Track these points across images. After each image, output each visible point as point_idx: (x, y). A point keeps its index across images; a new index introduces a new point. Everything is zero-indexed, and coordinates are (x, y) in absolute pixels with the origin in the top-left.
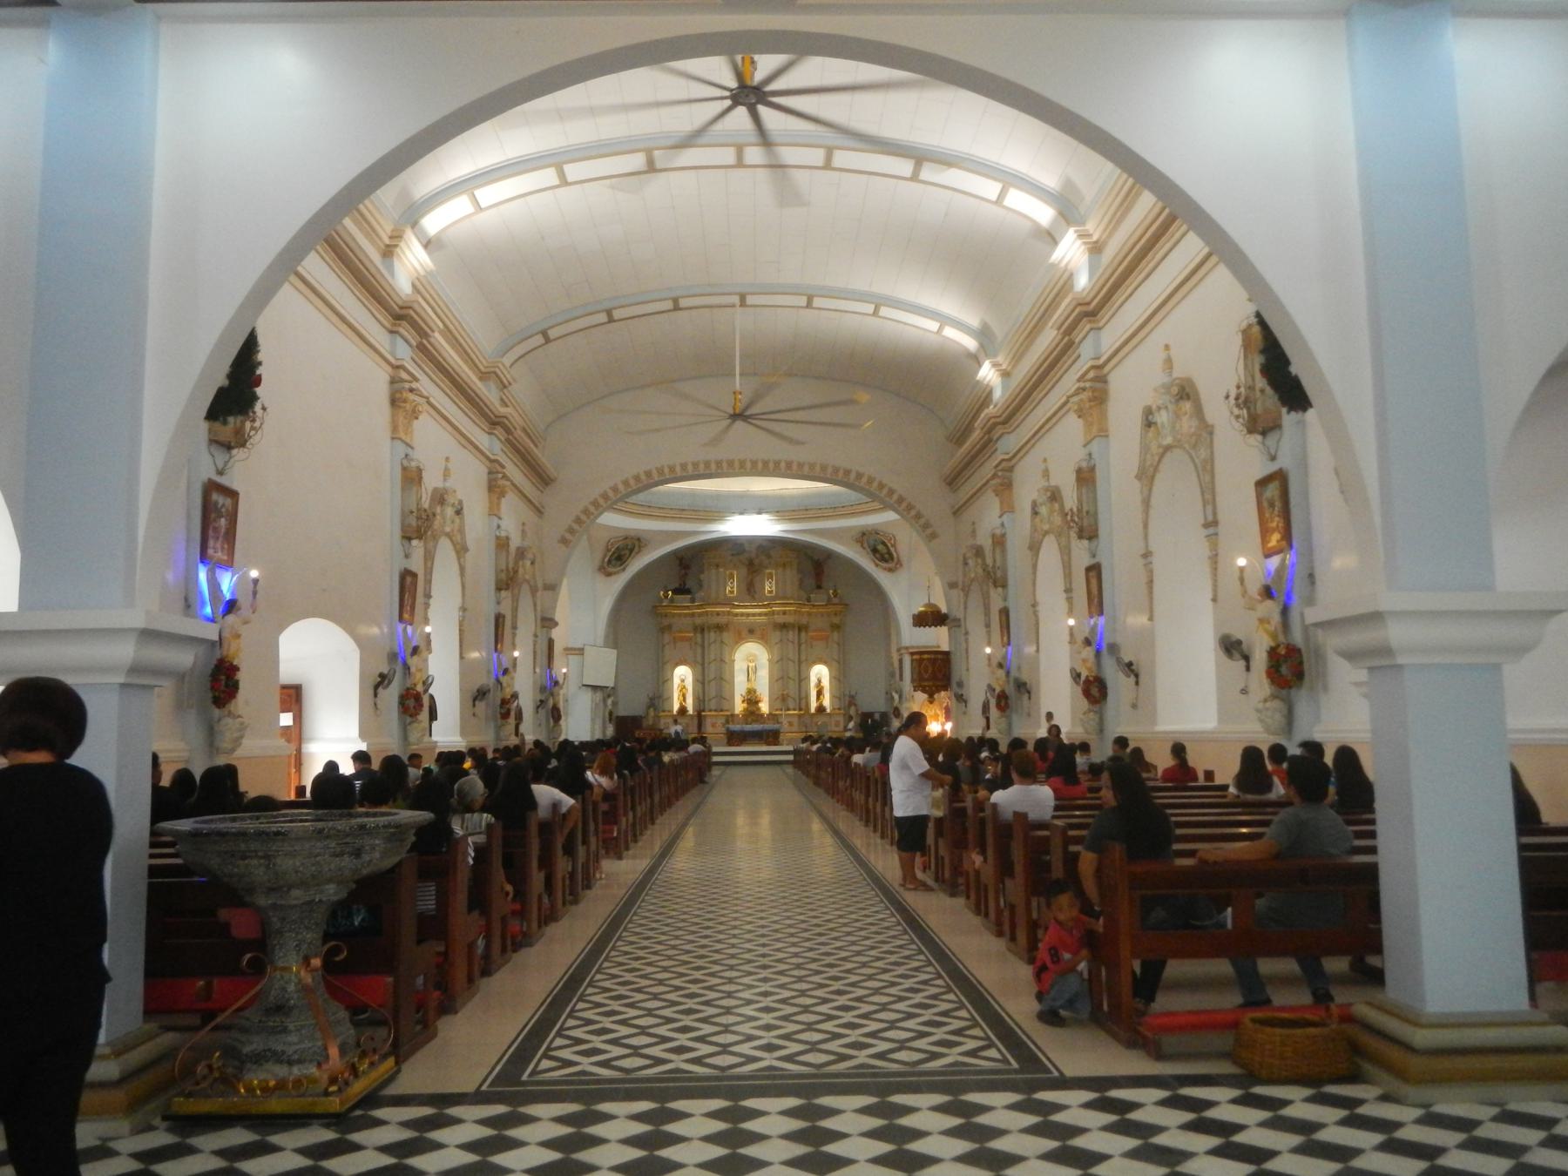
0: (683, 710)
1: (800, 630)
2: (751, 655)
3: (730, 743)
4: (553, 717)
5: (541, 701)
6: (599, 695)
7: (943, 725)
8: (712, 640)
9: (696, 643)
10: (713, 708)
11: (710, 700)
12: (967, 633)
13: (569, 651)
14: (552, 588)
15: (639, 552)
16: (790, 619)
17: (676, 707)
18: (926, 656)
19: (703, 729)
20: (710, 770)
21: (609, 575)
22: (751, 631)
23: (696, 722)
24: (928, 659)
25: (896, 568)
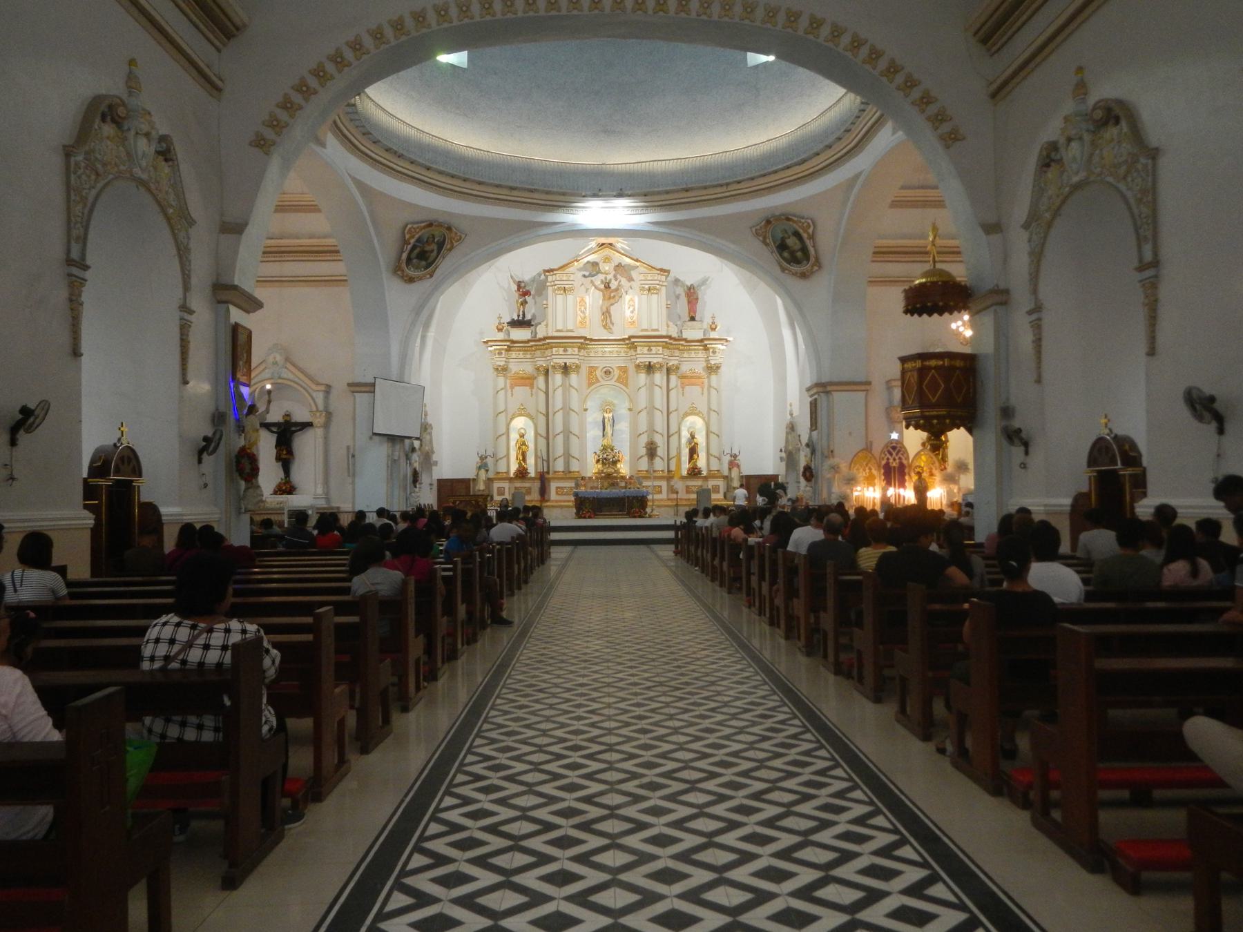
0: (522, 474)
1: (668, 370)
2: (609, 404)
3: (579, 515)
4: (240, 471)
5: (206, 439)
6: (398, 452)
7: (884, 490)
11: (555, 460)
12: (1037, 309)
13: (356, 387)
14: (234, 229)
15: (450, 250)
17: (514, 467)
18: (933, 363)
19: (546, 497)
20: (543, 558)
21: (411, 280)
23: (537, 485)
24: (936, 368)
25: (812, 273)
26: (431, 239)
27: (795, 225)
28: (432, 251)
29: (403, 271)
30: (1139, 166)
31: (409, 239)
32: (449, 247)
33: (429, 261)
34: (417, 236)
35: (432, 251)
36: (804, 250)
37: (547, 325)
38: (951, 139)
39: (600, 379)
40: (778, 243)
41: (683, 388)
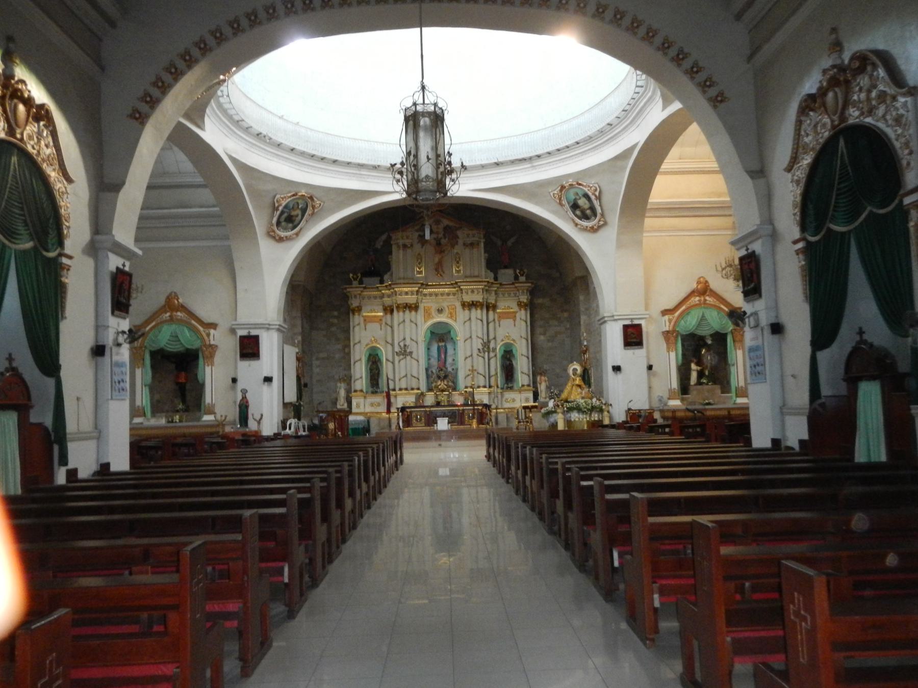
8: (401, 320)
9: (386, 324)
10: (404, 386)
11: (400, 380)
15: (313, 214)
16: (478, 298)
21: (280, 240)
22: (440, 311)
25: (600, 227)
26: (296, 206)
27: (585, 189)
28: (297, 216)
29: (274, 231)
30: (898, 105)
31: (278, 207)
32: (310, 212)
33: (296, 223)
34: (284, 203)
35: (297, 216)
36: (593, 209)
37: (391, 275)
38: (717, 101)
39: (433, 314)
40: (571, 204)
41: (499, 321)
